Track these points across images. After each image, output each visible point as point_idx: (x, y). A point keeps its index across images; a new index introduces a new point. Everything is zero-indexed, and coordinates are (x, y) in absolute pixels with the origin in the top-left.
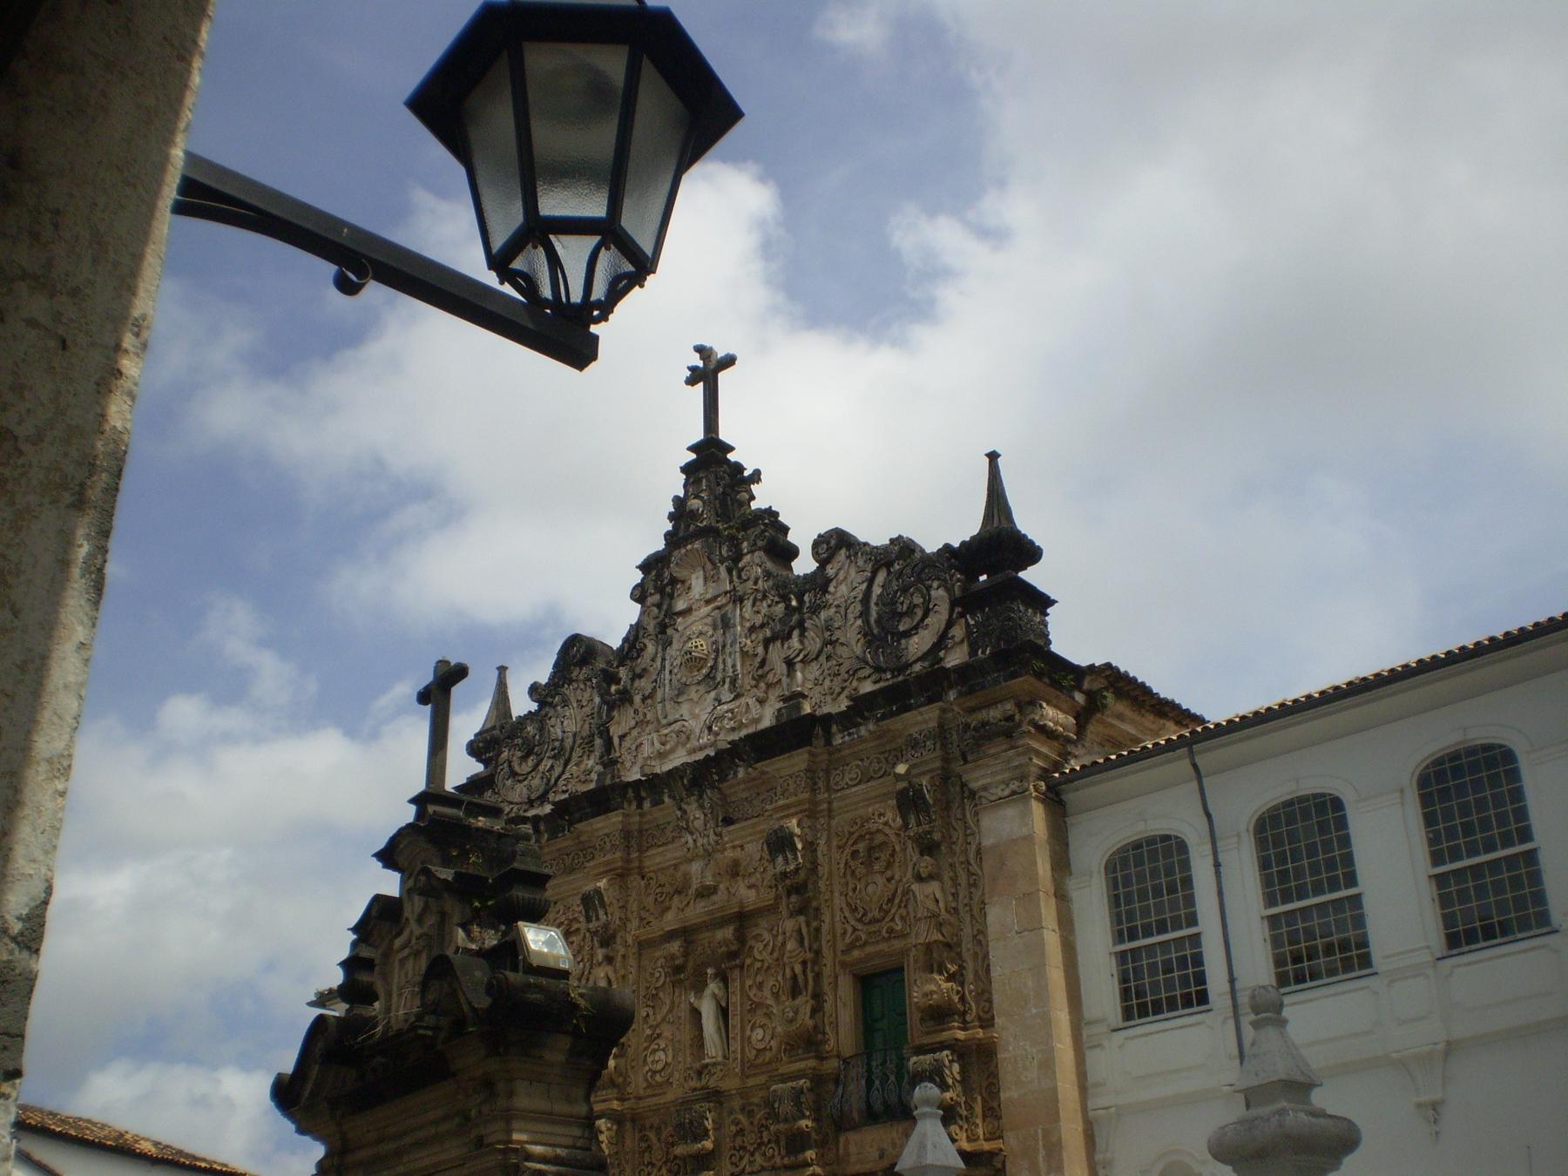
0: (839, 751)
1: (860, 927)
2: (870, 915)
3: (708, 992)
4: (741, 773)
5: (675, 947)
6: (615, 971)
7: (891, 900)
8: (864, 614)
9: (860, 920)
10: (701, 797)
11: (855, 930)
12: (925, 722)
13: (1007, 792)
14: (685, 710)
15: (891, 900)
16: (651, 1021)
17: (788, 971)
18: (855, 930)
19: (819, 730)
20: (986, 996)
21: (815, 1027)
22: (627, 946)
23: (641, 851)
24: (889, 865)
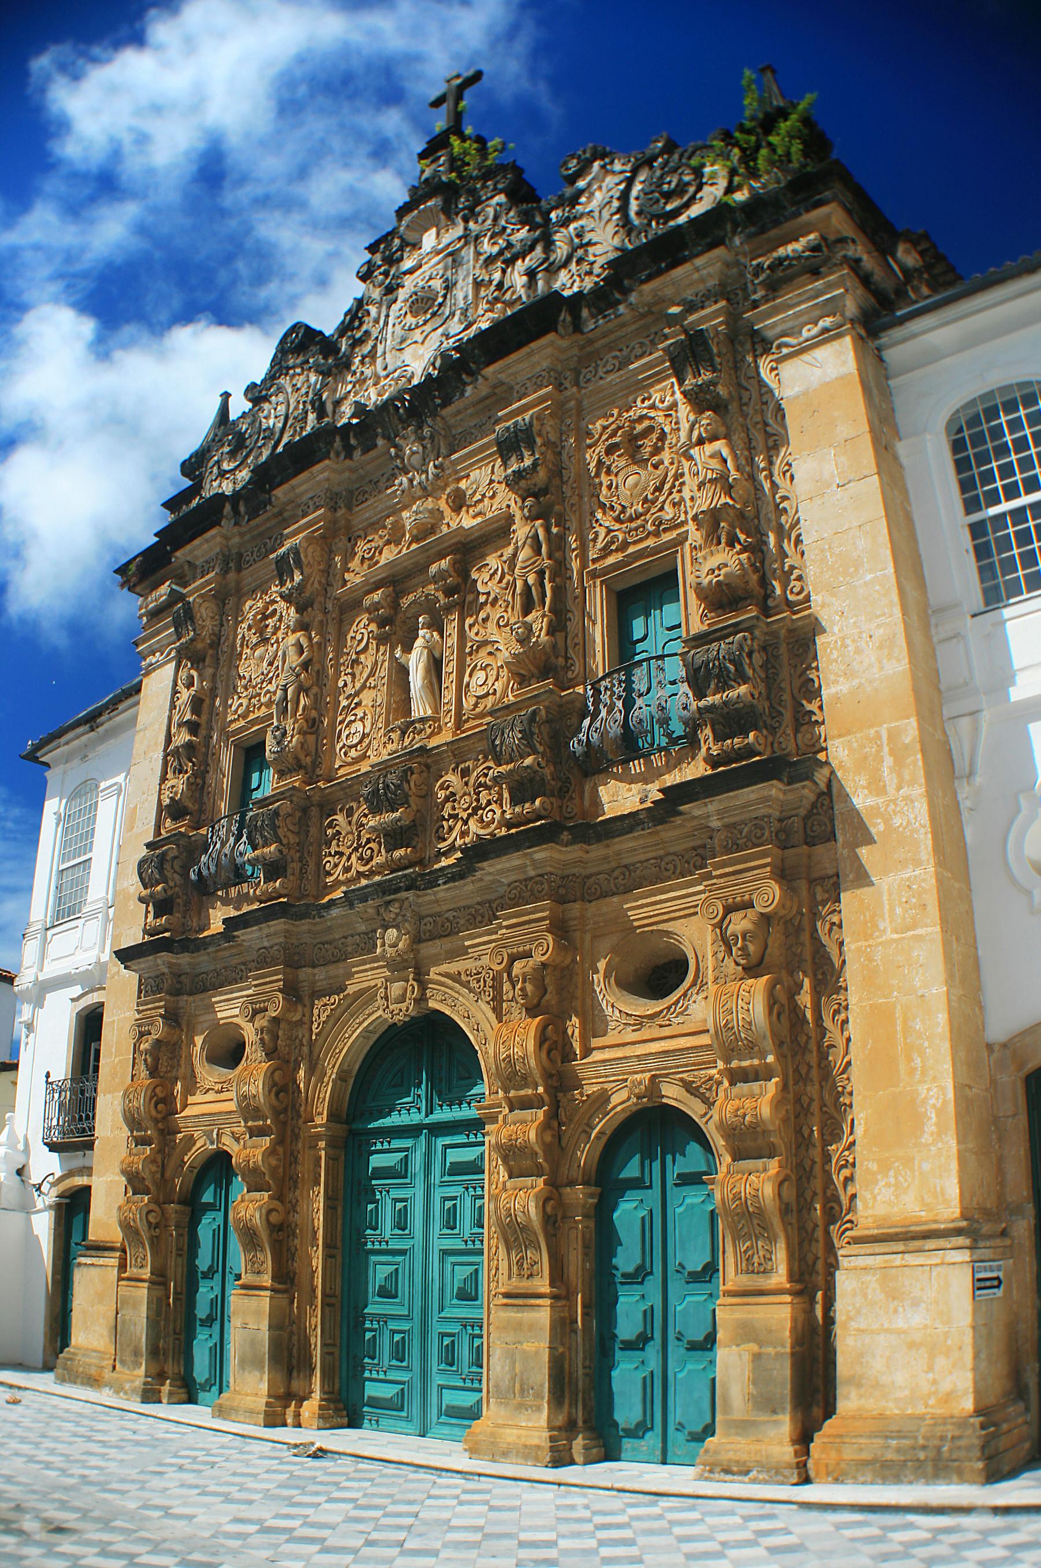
0: (591, 342)
1: (617, 526)
2: (630, 511)
3: (419, 642)
4: (469, 390)
5: (376, 596)
6: (310, 639)
7: (659, 489)
8: (623, 209)
9: (618, 520)
10: (420, 427)
11: (609, 531)
12: (702, 280)
13: (815, 331)
14: (407, 356)
15: (659, 489)
16: (349, 690)
17: (519, 584)
18: (609, 531)
19: (564, 316)
20: (796, 573)
21: (554, 646)
22: (325, 612)
23: (349, 508)
24: (657, 450)
